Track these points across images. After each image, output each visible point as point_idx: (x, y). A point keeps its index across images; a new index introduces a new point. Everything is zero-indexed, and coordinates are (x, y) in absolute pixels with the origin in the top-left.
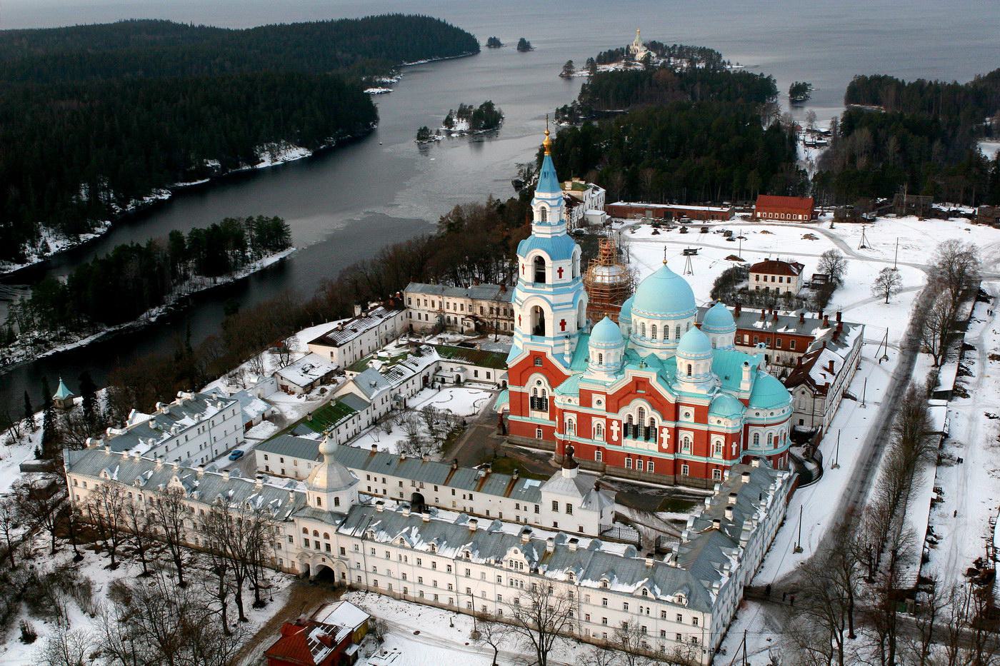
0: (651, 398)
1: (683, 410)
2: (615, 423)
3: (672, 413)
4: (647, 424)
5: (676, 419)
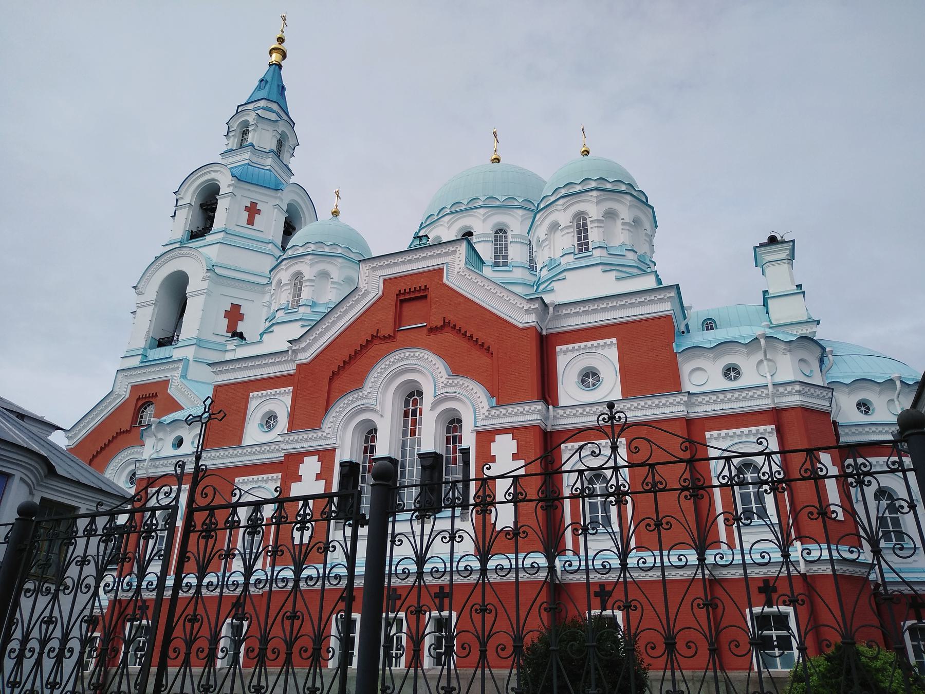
0: (448, 337)
1: (568, 362)
2: (310, 467)
3: (531, 376)
4: (430, 439)
5: (547, 391)
